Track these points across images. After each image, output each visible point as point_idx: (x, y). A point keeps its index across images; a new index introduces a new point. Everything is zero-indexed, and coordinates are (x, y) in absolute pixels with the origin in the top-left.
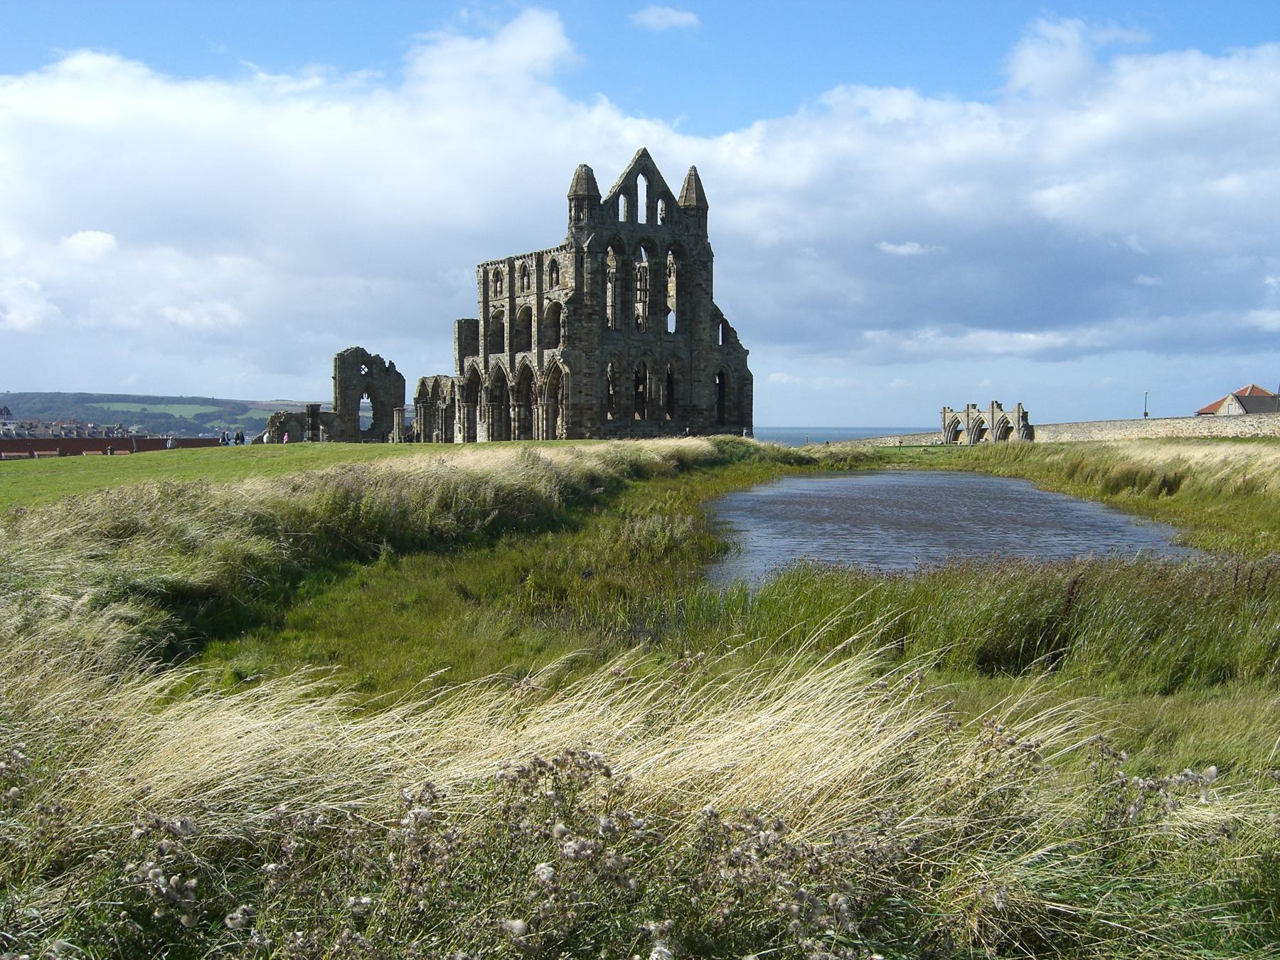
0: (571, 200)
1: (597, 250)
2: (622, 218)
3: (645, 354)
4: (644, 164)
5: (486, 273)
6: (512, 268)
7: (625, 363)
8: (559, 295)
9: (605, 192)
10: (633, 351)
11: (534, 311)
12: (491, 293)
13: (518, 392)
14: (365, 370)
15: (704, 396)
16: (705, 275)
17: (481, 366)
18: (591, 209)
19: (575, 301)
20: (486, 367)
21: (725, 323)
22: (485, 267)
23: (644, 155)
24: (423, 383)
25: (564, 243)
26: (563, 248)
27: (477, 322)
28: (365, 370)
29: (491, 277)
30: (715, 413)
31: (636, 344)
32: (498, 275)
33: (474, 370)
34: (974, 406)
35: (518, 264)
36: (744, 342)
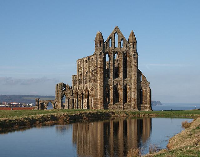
2: (110, 46)
4: (117, 31)
6: (83, 61)
8: (93, 68)
11: (88, 73)
20: (78, 88)
21: (142, 74)
33: (76, 89)
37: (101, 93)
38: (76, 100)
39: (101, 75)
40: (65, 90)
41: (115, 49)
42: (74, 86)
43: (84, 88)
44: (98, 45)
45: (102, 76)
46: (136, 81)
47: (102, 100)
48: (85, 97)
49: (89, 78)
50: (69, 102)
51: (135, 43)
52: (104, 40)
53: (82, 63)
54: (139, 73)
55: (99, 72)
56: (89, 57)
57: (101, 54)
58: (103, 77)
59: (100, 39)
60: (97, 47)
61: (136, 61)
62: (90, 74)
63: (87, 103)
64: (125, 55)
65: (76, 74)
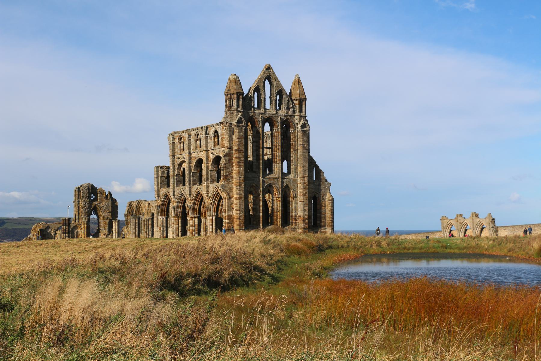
0: (227, 95)
2: (256, 106)
5: (174, 138)
6: (190, 135)
11: (204, 161)
13: (194, 209)
19: (228, 155)
21: (317, 167)
23: (269, 68)
24: (130, 205)
25: (222, 120)
26: (222, 123)
29: (177, 140)
34: (461, 216)
35: (193, 133)
37: (239, 204)
38: (165, 220)
39: (239, 166)
40: (96, 200)
41: (265, 112)
42: (158, 190)
43: (190, 195)
45: (242, 169)
46: (306, 180)
47: (242, 218)
48: (193, 214)
49: (207, 173)
50: (139, 224)
51: (303, 101)
52: (244, 93)
54: (311, 164)
55: (235, 160)
56: (207, 128)
57: (239, 122)
58: (245, 170)
59: (238, 91)
60: (229, 107)
61: (306, 139)
62: (210, 164)
63: (197, 227)
64: (287, 125)
65: (167, 162)
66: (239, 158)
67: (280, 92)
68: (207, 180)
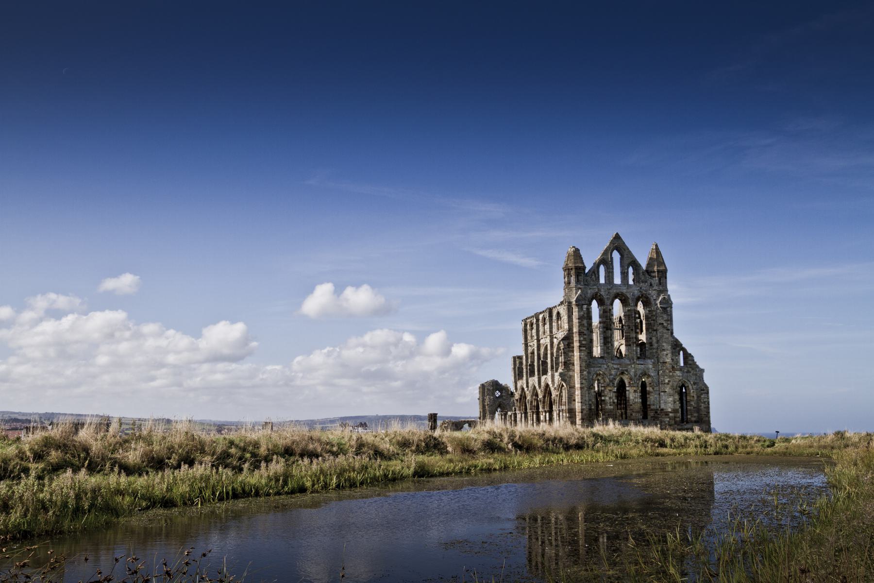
0: (565, 270)
1: (583, 303)
2: (602, 281)
3: (622, 373)
4: (618, 244)
5: (526, 325)
6: (538, 320)
7: (607, 380)
8: (560, 335)
9: (589, 266)
10: (613, 372)
11: (549, 348)
12: (529, 338)
13: (544, 402)
14: (498, 394)
15: (668, 402)
16: (665, 316)
17: (525, 386)
18: (578, 276)
19: (568, 339)
20: (527, 386)
21: (684, 350)
22: (525, 320)
23: (617, 237)
25: (562, 300)
26: (562, 303)
27: (520, 358)
28: (498, 394)
30: (679, 414)
31: (615, 366)
32: (532, 325)
33: (523, 389)
35: (541, 316)
36: (700, 362)
39: (580, 351)
44: (573, 279)
47: (585, 412)
48: (543, 408)
49: (552, 360)
52: (584, 268)
53: (535, 326)
55: (576, 344)
65: (522, 353)
66: (580, 341)
67: (635, 264)
68: (552, 368)
